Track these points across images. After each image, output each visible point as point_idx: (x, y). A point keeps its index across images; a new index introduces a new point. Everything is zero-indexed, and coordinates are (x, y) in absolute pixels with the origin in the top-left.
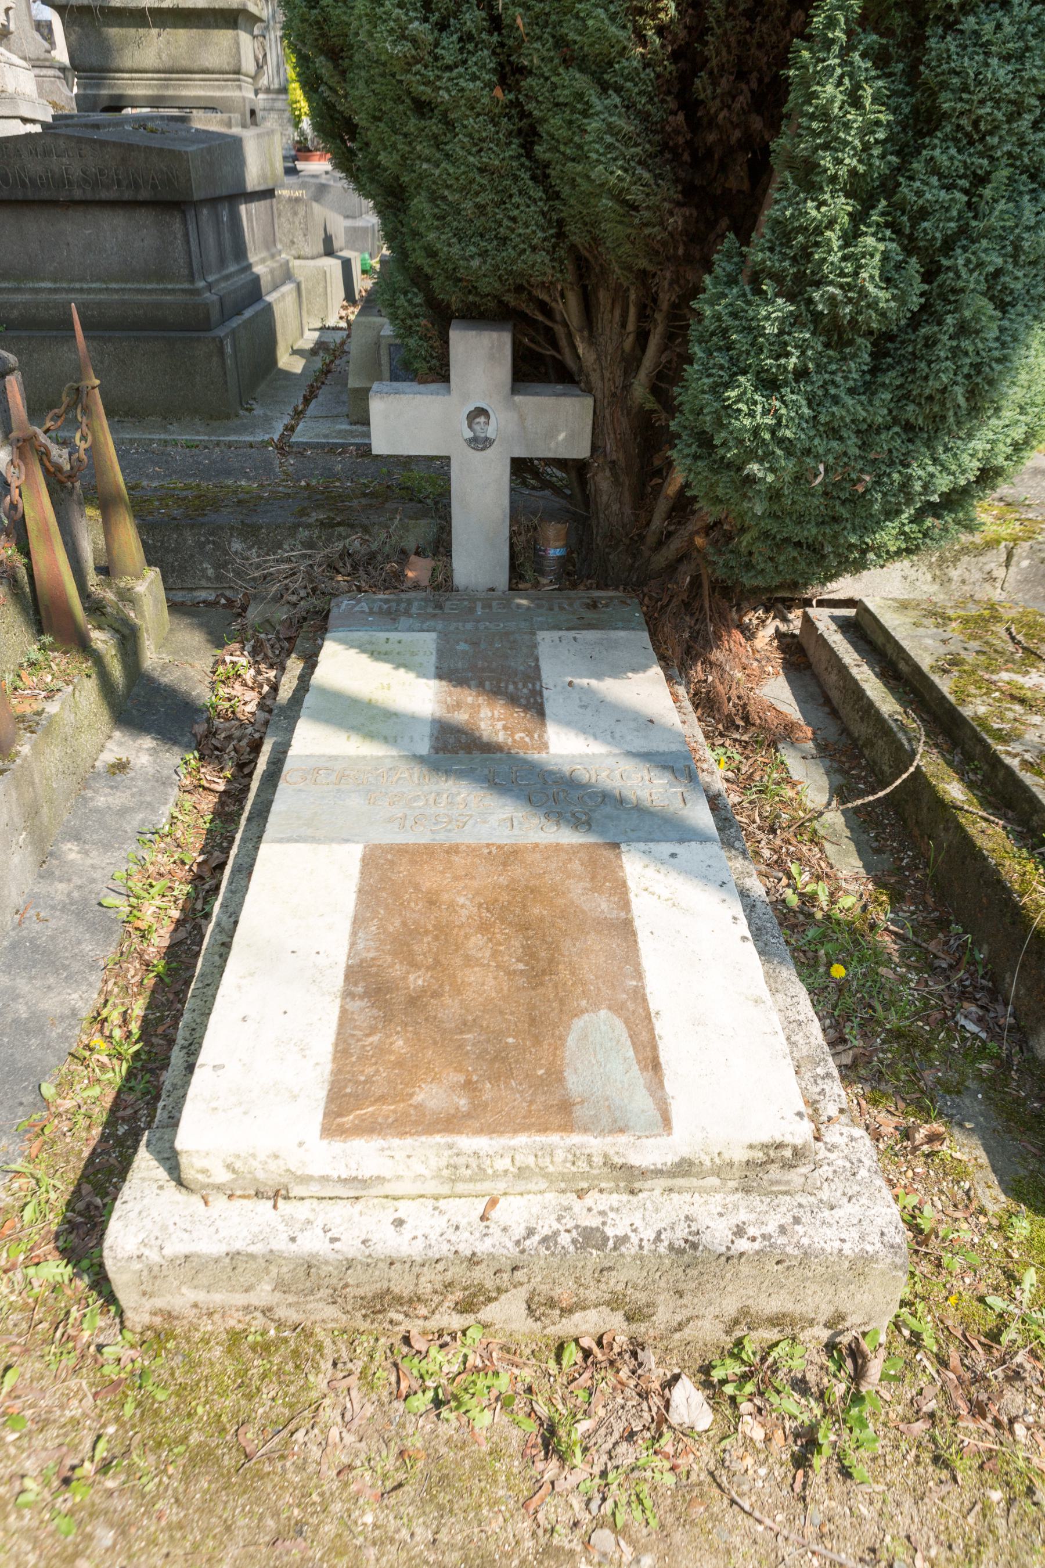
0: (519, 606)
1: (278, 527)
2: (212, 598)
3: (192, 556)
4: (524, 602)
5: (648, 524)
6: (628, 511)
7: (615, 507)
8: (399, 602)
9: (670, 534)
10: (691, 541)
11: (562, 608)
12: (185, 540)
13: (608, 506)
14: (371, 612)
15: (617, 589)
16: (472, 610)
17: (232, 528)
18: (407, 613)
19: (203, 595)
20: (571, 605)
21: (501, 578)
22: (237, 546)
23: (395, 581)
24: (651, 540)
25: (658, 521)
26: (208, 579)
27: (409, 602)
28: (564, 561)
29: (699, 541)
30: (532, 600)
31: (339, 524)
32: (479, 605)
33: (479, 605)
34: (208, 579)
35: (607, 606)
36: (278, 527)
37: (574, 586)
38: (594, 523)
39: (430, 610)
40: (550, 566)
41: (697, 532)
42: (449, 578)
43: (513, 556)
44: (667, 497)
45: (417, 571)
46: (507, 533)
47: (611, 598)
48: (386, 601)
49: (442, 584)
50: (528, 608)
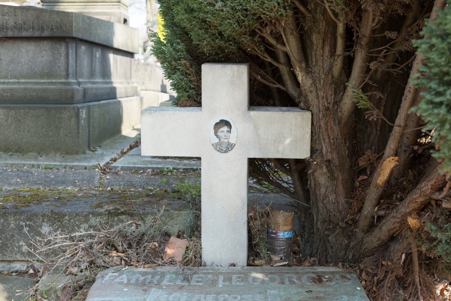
0: (255, 279)
1: (77, 215)
2: (24, 268)
3: (13, 236)
4: (260, 276)
5: (360, 210)
6: (342, 200)
7: (332, 197)
8: (154, 275)
9: (380, 218)
10: (404, 222)
11: (292, 282)
12: (9, 224)
13: (325, 196)
14: (129, 284)
15: (336, 265)
16: (214, 283)
17: (44, 215)
18: (159, 285)
19: (18, 266)
20: (299, 279)
21: (241, 255)
22: (45, 229)
23: (155, 257)
24: (363, 223)
25: (369, 208)
26: (23, 254)
27: (163, 275)
28: (292, 242)
29: (412, 222)
30: (267, 274)
31: (122, 213)
32: (221, 278)
33: (221, 278)
34: (23, 254)
35: (330, 280)
36: (77, 215)
37: (300, 263)
38: (314, 211)
39: (179, 282)
40: (281, 246)
41: (410, 214)
42: (198, 255)
43: (250, 238)
44: (377, 186)
45: (175, 249)
46: (246, 219)
47: (333, 273)
48: (144, 274)
49: (193, 260)
50: (263, 282)
